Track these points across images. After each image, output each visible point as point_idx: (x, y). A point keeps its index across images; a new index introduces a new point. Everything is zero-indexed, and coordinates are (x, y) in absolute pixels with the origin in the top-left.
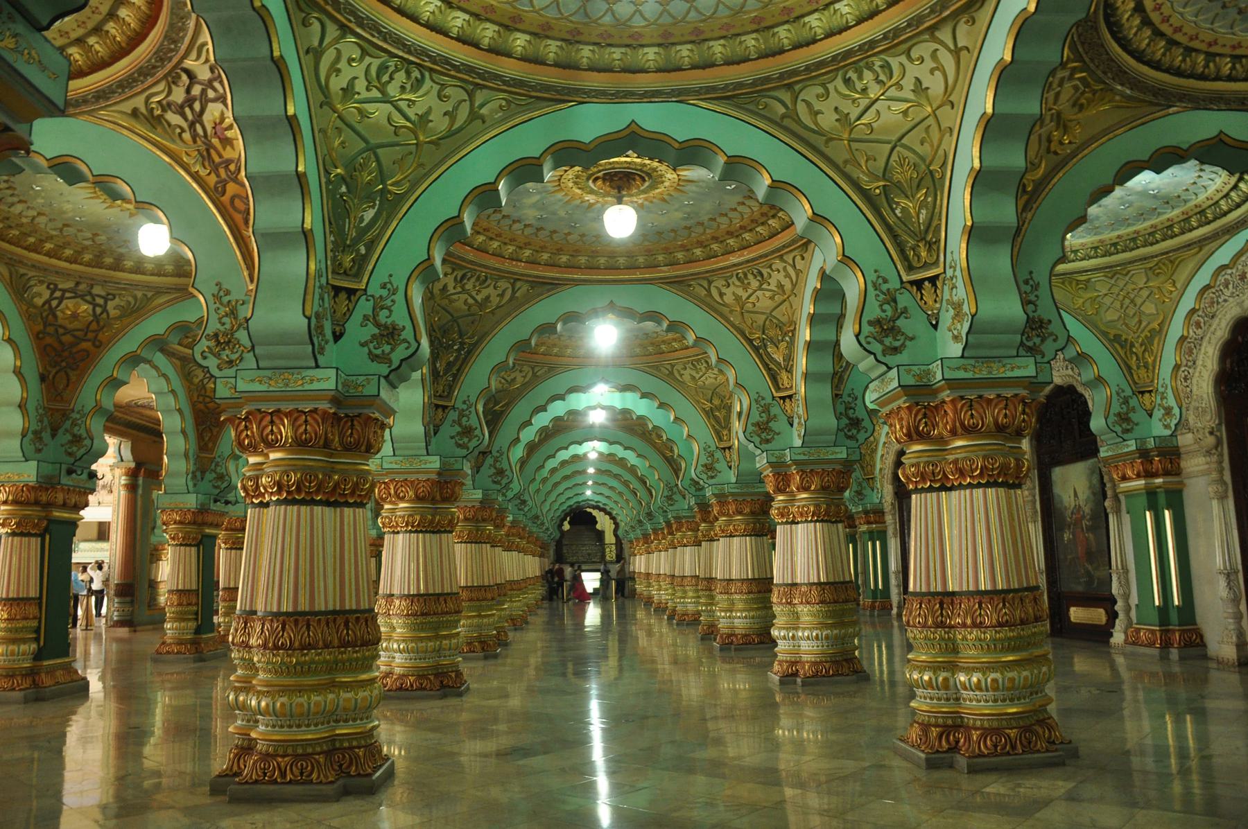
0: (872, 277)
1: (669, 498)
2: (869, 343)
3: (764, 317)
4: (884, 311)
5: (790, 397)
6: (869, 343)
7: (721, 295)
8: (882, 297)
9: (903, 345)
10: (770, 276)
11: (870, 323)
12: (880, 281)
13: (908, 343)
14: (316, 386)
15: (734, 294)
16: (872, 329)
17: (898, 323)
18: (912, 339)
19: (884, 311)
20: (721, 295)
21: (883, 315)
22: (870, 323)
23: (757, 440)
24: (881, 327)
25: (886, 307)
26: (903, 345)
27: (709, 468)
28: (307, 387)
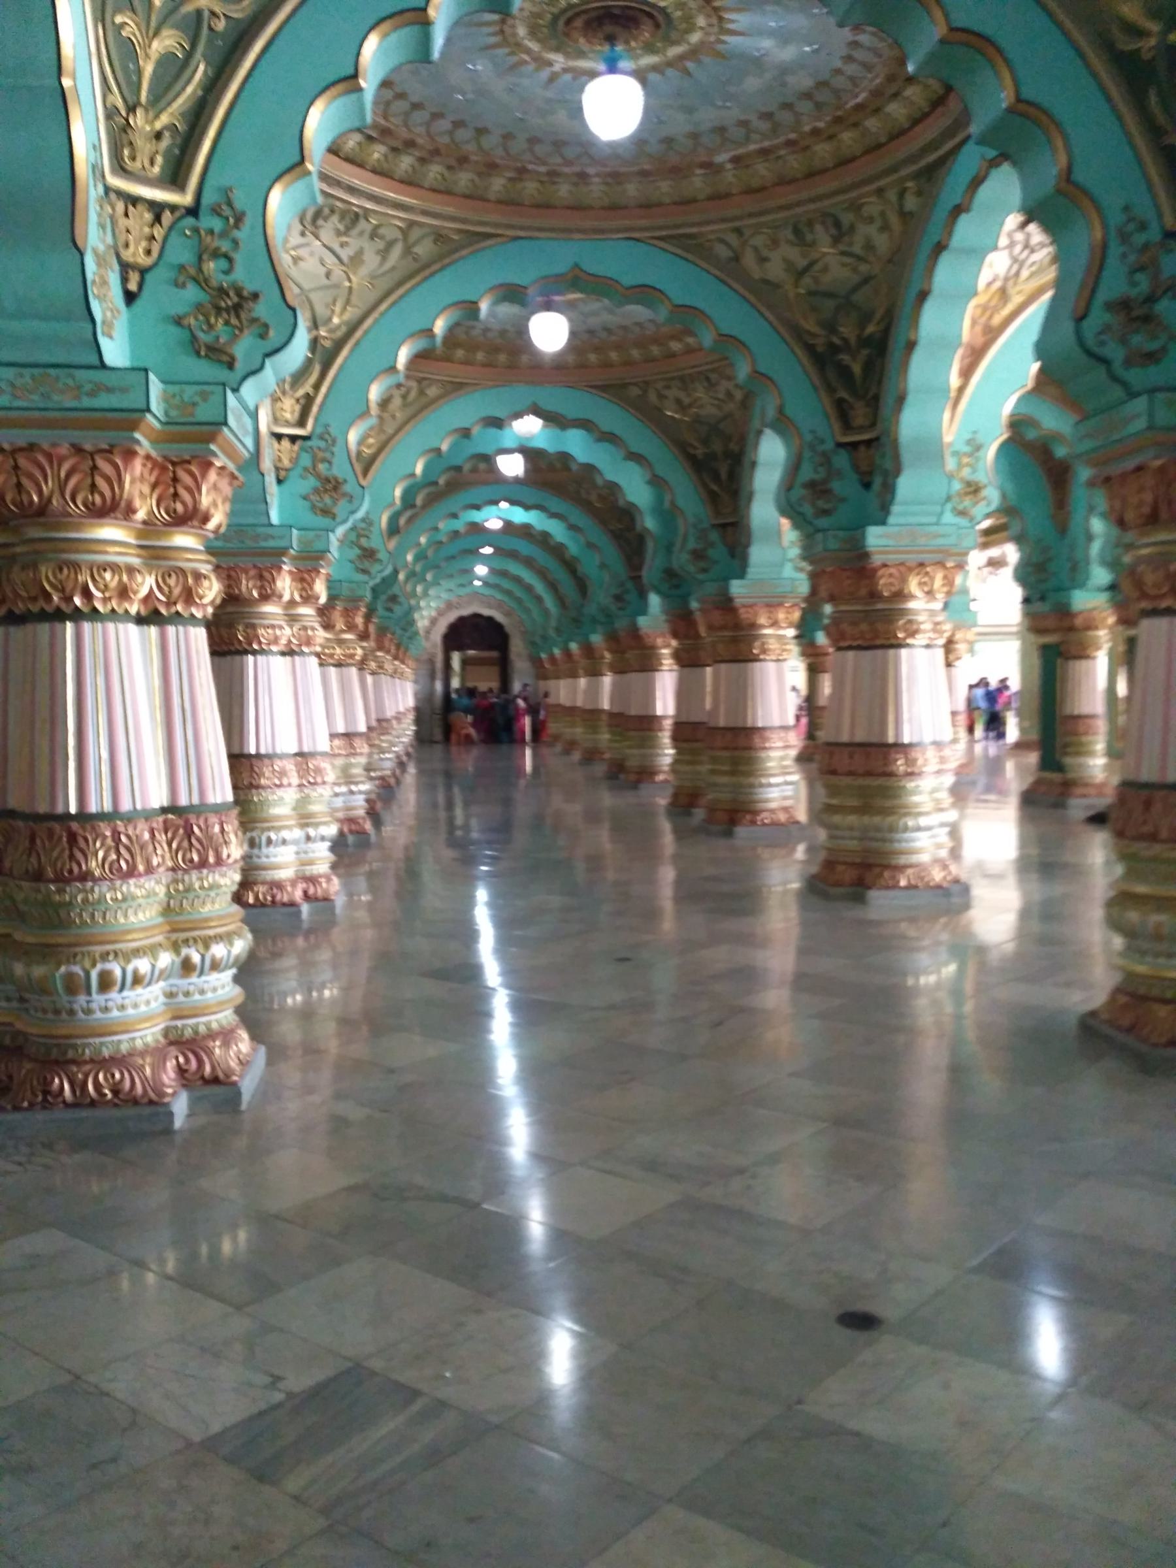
0: (1116, 218)
3: (830, 304)
5: (869, 443)
7: (763, 260)
8: (1132, 258)
9: (1164, 350)
10: (852, 228)
15: (785, 260)
16: (1107, 317)
20: (763, 260)
21: (1133, 293)
22: (1109, 306)
23: (808, 509)
28: (87, 402)
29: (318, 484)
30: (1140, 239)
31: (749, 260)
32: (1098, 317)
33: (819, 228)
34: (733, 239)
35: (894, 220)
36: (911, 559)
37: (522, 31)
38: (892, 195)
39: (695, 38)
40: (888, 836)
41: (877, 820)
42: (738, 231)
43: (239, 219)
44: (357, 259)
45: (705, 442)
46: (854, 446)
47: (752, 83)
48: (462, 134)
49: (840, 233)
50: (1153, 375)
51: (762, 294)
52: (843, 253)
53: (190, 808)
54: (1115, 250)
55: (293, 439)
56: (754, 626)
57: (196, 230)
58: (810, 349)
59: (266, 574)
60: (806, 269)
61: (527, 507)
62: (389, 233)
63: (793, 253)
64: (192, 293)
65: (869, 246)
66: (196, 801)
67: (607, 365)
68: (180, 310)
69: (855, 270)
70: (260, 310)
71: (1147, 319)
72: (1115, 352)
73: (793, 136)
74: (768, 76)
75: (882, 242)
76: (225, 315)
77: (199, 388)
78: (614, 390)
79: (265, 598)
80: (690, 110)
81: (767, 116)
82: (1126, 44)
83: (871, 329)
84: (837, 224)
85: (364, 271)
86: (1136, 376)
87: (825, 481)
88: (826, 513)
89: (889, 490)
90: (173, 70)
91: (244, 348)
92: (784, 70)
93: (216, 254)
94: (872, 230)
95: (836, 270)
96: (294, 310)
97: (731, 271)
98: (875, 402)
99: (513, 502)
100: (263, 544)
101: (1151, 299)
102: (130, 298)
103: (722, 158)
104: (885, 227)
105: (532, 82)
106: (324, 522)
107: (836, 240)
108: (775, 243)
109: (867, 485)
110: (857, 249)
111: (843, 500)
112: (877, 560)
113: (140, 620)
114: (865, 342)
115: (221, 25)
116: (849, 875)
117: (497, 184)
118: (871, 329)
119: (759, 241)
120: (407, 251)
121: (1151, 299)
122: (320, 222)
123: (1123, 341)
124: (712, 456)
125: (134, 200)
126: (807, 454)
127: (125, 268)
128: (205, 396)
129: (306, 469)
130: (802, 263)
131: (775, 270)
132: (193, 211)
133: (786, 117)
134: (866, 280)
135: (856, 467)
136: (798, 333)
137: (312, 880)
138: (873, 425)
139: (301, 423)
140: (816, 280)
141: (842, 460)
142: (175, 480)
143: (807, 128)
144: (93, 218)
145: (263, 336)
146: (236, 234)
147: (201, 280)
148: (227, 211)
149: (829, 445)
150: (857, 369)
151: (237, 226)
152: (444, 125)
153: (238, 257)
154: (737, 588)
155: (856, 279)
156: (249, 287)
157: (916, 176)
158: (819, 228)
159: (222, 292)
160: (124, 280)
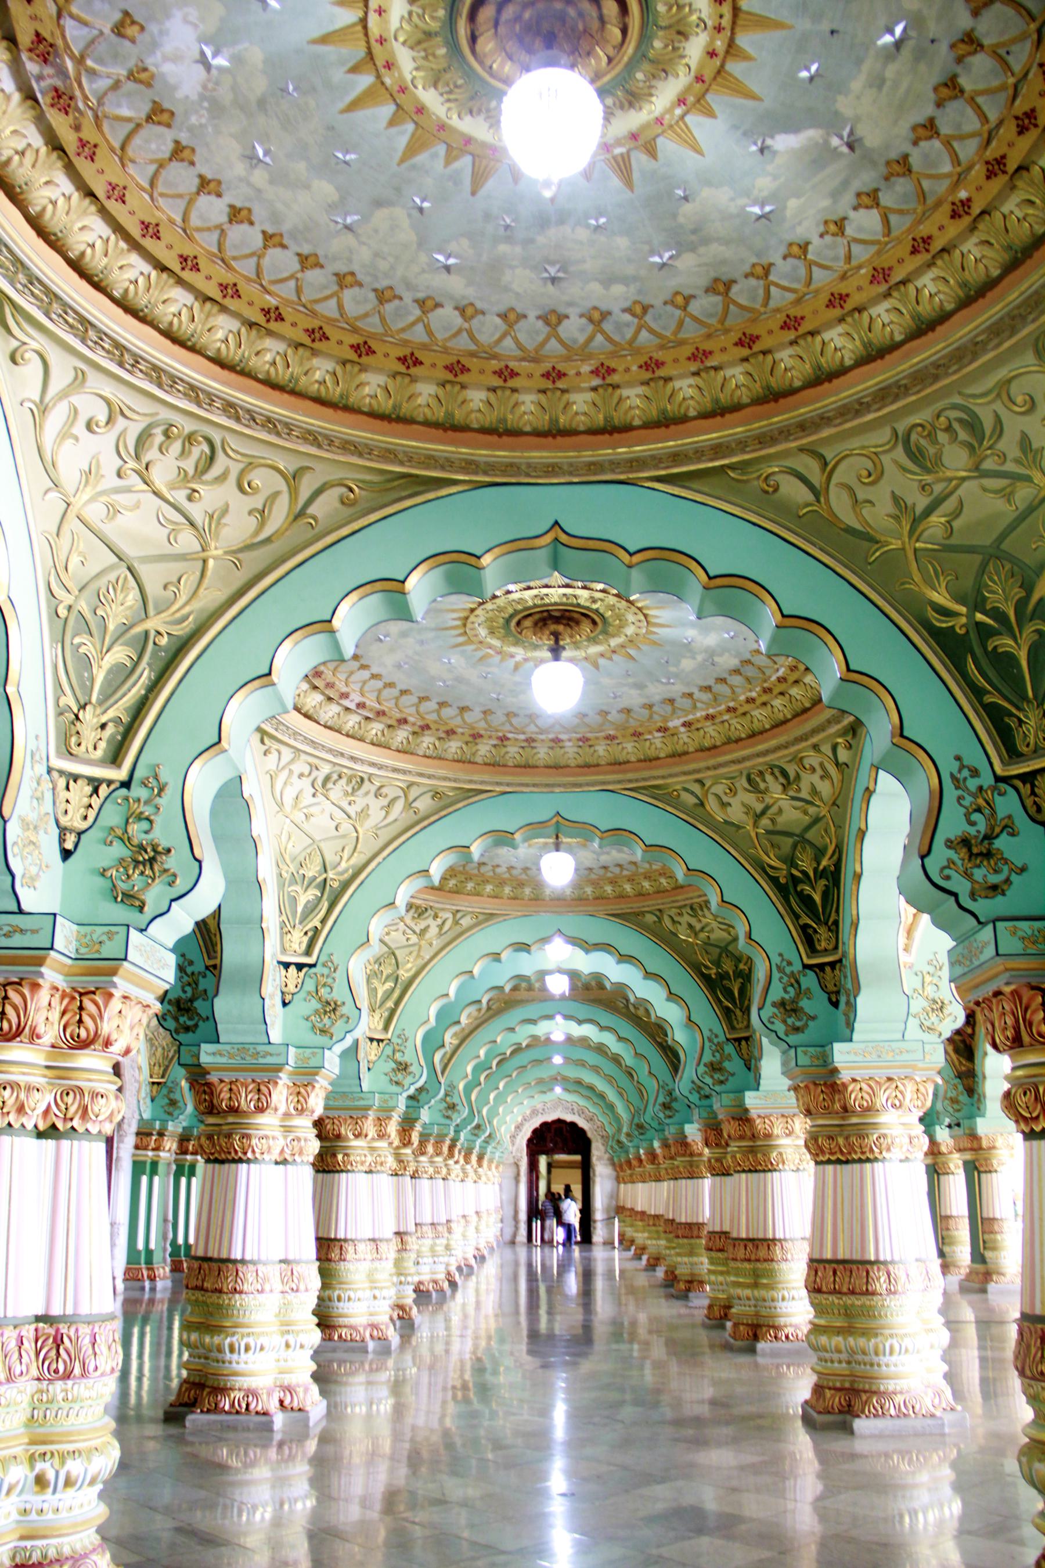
0: (948, 766)
1: (666, 1106)
2: (948, 878)
3: (790, 841)
4: (972, 824)
5: (832, 965)
6: (948, 878)
8: (968, 801)
10: (798, 777)
11: (949, 844)
12: (966, 773)
13: (1014, 877)
14: (17, 941)
15: (744, 805)
16: (951, 854)
17: (998, 843)
18: (1023, 870)
19: (972, 824)
20: (724, 805)
21: (972, 831)
22: (949, 844)
23: (780, 1028)
24: (970, 850)
25: (976, 817)
26: (1008, 881)
27: (714, 1068)
29: (319, 1006)
30: (972, 784)
31: (712, 805)
32: (941, 854)
33: (769, 778)
34: (696, 788)
35: (832, 770)
36: (880, 1074)
37: (483, 632)
38: (826, 749)
39: (630, 630)
40: (875, 1359)
41: (862, 1342)
42: (700, 782)
43: (161, 790)
44: (364, 813)
45: (717, 963)
46: (821, 967)
47: (687, 664)
48: (447, 712)
49: (788, 782)
50: (997, 905)
51: (726, 834)
52: (793, 798)
53: (62, 1319)
54: (951, 793)
55: (300, 967)
56: (768, 1136)
57: (127, 799)
58: (774, 881)
59: (263, 1089)
60: (763, 812)
61: (580, 1022)
62: (391, 792)
63: (750, 799)
64: (119, 850)
65: (814, 791)
66: (69, 1311)
67: (622, 896)
68: (106, 864)
69: (806, 813)
70: (171, 862)
71: (988, 855)
72: (961, 886)
73: (732, 704)
74: (700, 658)
75: (825, 788)
76: (141, 867)
77: (106, 929)
78: (630, 918)
79: (260, 1110)
80: (640, 686)
81: (708, 688)
82: (942, 623)
83: (824, 863)
84: (784, 773)
85: (370, 823)
86: (983, 907)
87: (794, 1001)
88: (797, 1030)
89: (852, 1007)
90: (122, 675)
91: (155, 895)
92: (711, 653)
93: (140, 817)
94: (815, 778)
95: (791, 815)
96: (200, 862)
97: (696, 815)
98: (835, 927)
99: (567, 1017)
100: (262, 1061)
101: (989, 837)
102: (66, 854)
103: (675, 723)
104: (825, 776)
105: (500, 671)
106: (322, 1040)
107: (785, 788)
108: (733, 791)
109: (835, 1004)
110: (804, 794)
111: (813, 1018)
112: (845, 1076)
113: (40, 1135)
114: (821, 874)
115: (164, 641)
116: (836, 1400)
117: (484, 749)
118: (824, 863)
119: (719, 789)
120: (409, 805)
121: (989, 837)
122: (330, 785)
123: (967, 875)
124: (723, 976)
125: (76, 778)
126: (776, 975)
127: (63, 831)
128: (110, 936)
129: (309, 993)
130: (759, 807)
131: (736, 813)
132: (126, 784)
133: (720, 688)
134: (817, 820)
135: (823, 988)
136: (762, 868)
137: (289, 1389)
138: (836, 948)
139: (308, 952)
140: (773, 821)
141: (809, 980)
142: (81, 1008)
143: (742, 698)
144: (26, 791)
145: (171, 884)
146: (158, 800)
147: (125, 839)
148: (153, 783)
149: (797, 966)
150: (817, 898)
151: (159, 795)
152: (432, 705)
153: (158, 820)
154: (751, 1099)
155: (807, 819)
156: (164, 844)
157: (843, 733)
158: (769, 778)
159: (142, 848)
160: (62, 840)
